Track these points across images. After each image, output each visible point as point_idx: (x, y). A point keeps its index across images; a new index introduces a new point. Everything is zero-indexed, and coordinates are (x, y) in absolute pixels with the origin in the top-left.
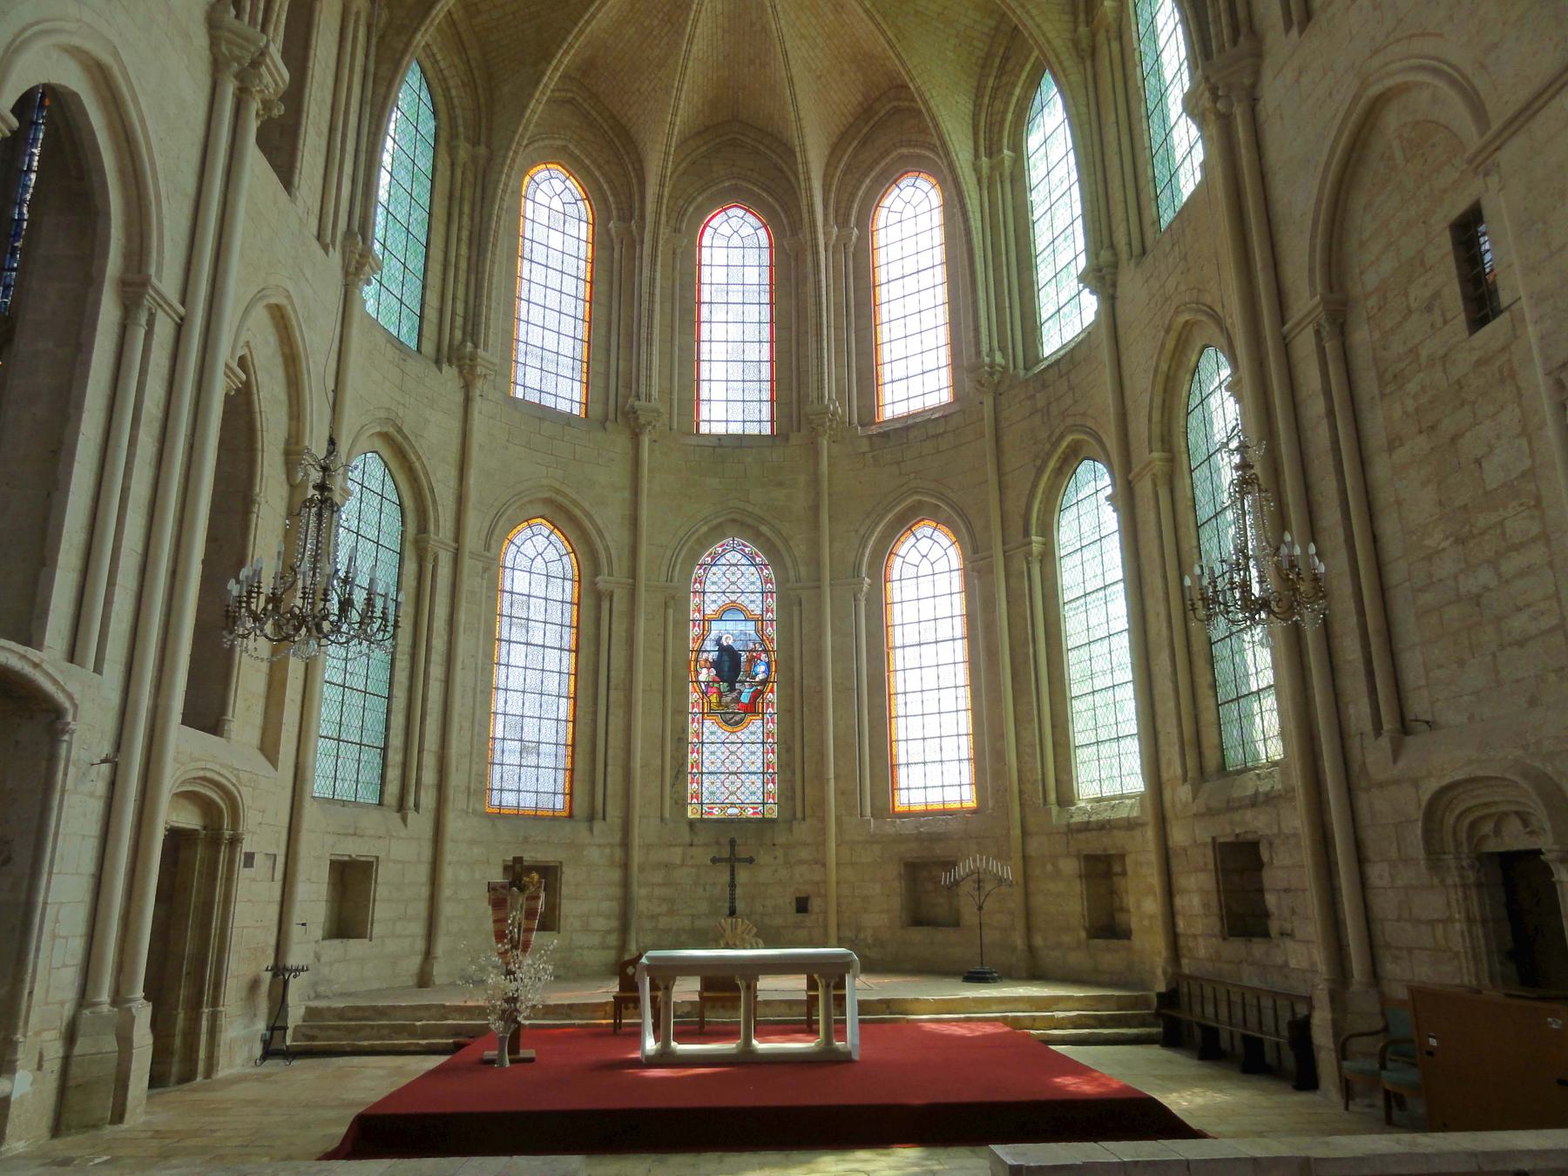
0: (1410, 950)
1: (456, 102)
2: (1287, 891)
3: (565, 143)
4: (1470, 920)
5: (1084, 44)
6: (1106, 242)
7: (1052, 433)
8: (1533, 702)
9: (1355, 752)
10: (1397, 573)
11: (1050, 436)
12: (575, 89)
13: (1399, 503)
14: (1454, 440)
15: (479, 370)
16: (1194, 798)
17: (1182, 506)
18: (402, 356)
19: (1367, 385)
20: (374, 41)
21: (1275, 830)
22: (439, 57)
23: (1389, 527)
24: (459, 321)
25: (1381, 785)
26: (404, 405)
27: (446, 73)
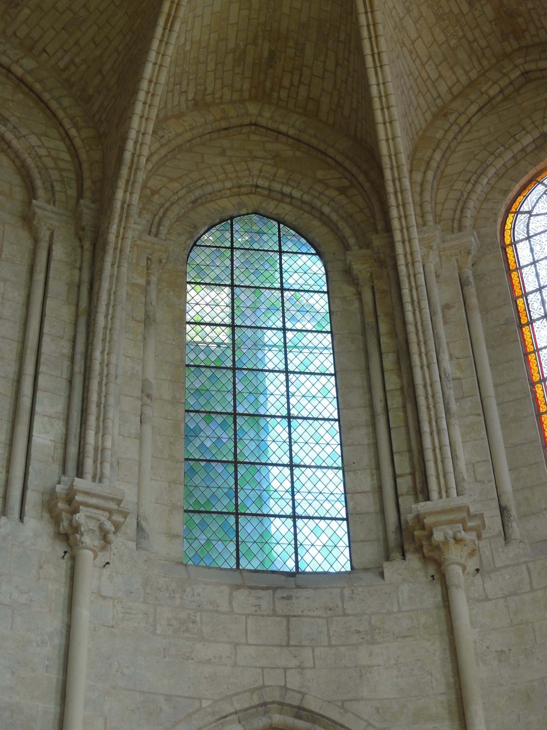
1: (334, 217)
3: (536, 134)
12: (519, 61)
15: (438, 536)
18: (279, 594)
20: (87, 245)
22: (287, 190)
24: (404, 484)
26: (301, 668)
27: (306, 198)
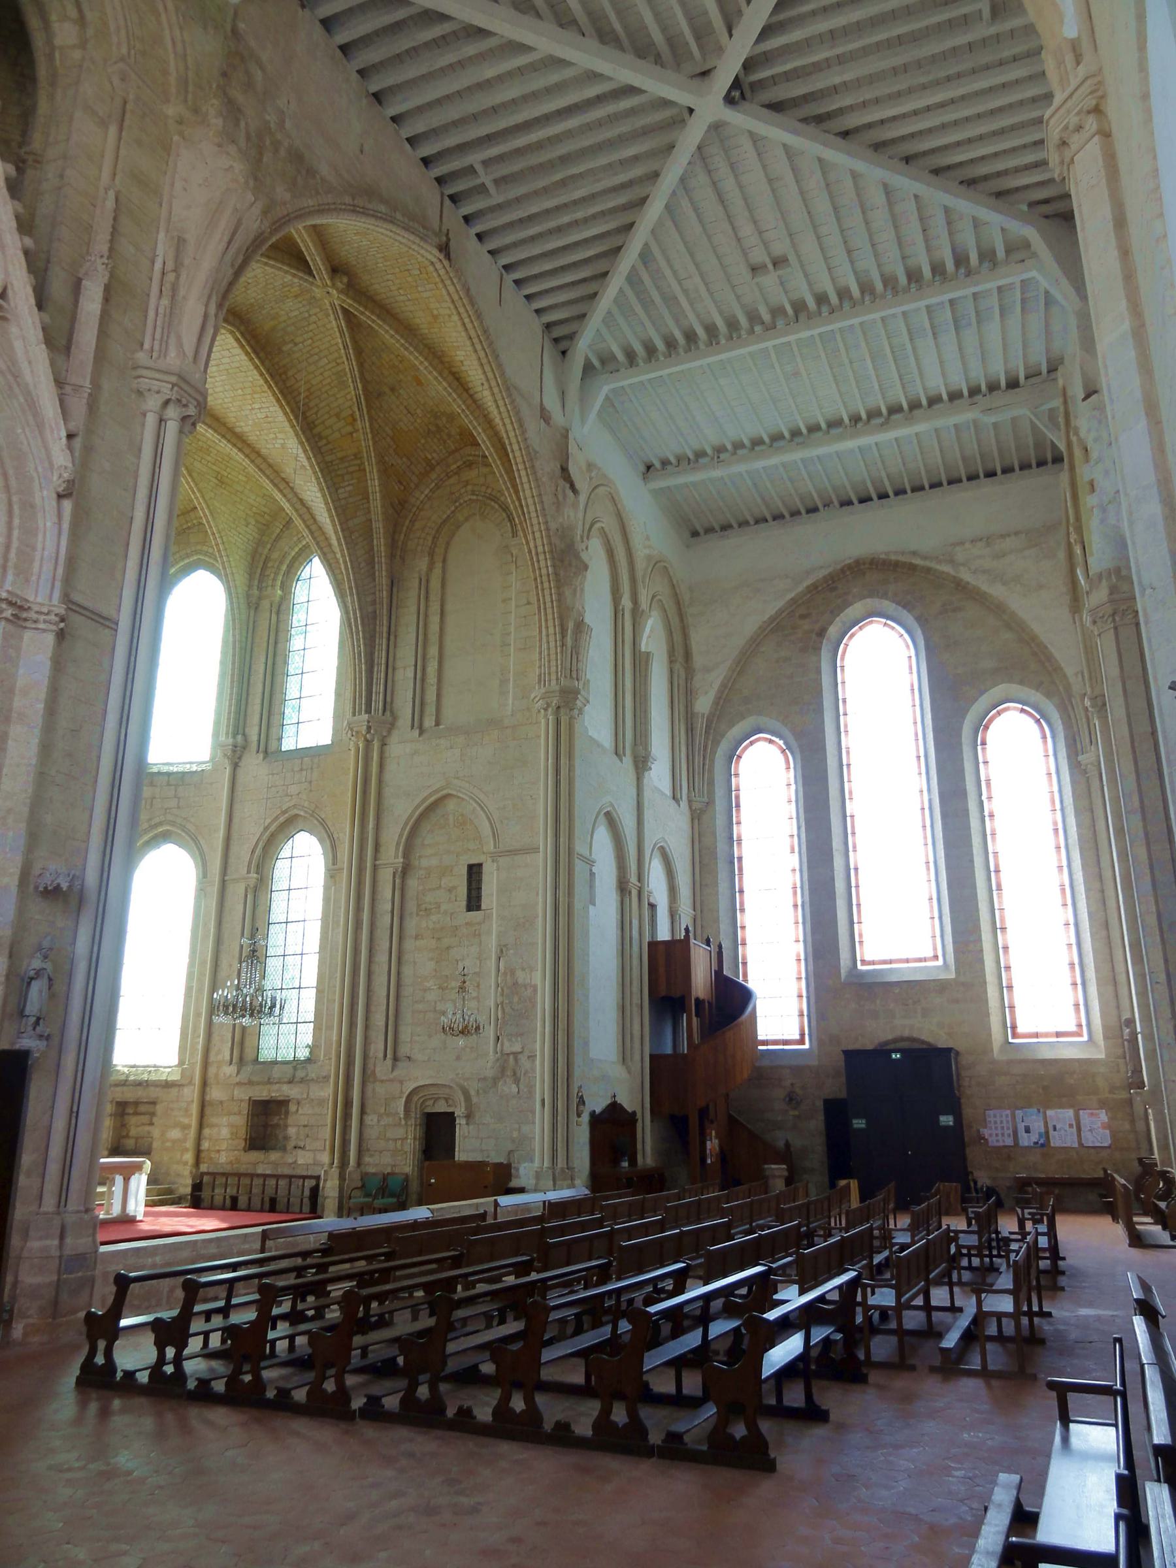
0: (381, 1152)
2: (305, 1126)
4: (415, 1138)
5: (254, 600)
6: (241, 731)
7: (150, 819)
8: (458, 1058)
9: (370, 1066)
10: (407, 991)
11: (150, 819)
13: (415, 963)
14: (448, 948)
16: (238, 1073)
17: (260, 909)
19: (411, 906)
21: (305, 1096)
23: (407, 971)
25: (382, 1081)
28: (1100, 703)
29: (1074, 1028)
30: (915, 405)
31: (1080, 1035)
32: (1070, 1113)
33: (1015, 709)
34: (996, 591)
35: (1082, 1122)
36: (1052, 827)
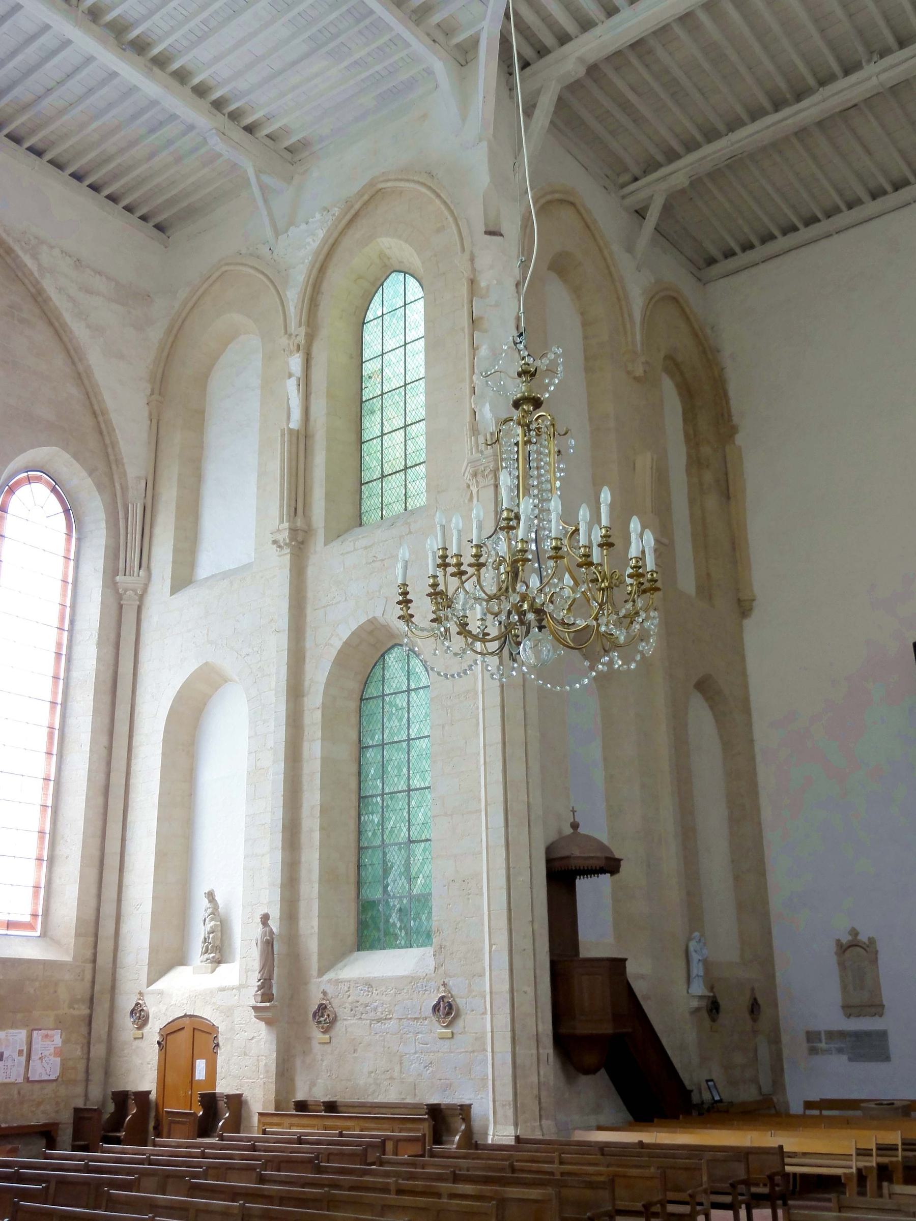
28: (300, 539)
29: (27, 918)
30: (160, 62)
31: (30, 926)
32: (22, 1034)
33: (47, 484)
34: (79, 331)
35: (34, 1047)
36: (53, 648)
